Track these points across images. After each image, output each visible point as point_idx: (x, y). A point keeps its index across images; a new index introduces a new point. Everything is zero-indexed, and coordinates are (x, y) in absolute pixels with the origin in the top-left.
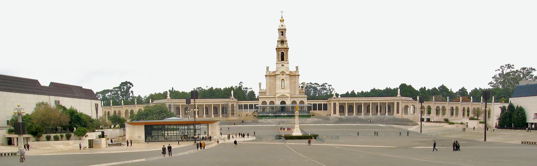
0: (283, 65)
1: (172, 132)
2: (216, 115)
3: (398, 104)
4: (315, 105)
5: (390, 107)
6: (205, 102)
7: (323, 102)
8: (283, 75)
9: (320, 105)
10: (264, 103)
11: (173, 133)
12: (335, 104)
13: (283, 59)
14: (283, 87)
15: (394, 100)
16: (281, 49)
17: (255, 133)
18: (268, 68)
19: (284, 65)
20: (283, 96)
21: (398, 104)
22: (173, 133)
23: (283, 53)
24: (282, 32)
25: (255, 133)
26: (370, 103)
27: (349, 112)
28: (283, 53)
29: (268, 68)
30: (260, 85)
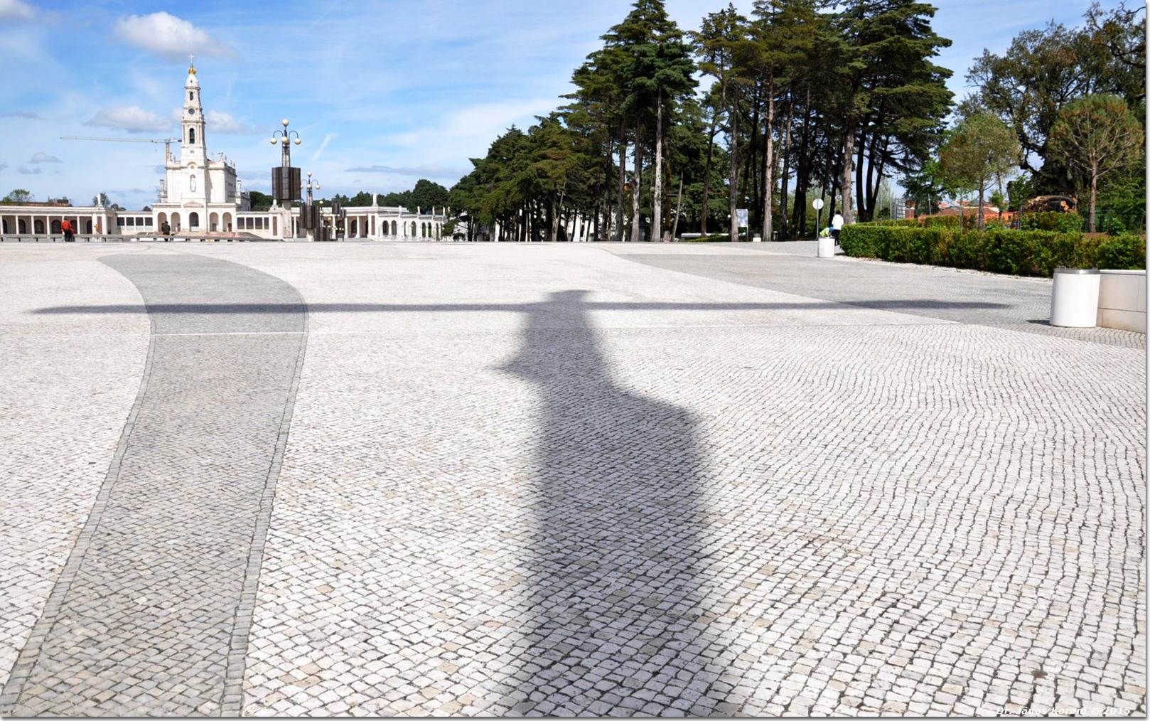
0: (192, 152)
3: (373, 217)
4: (250, 220)
7: (262, 215)
8: (192, 167)
9: (259, 220)
10: (162, 216)
12: (275, 219)
13: (192, 141)
15: (367, 212)
19: (195, 150)
20: (192, 204)
21: (373, 217)
23: (192, 130)
24: (191, 93)
28: (192, 130)
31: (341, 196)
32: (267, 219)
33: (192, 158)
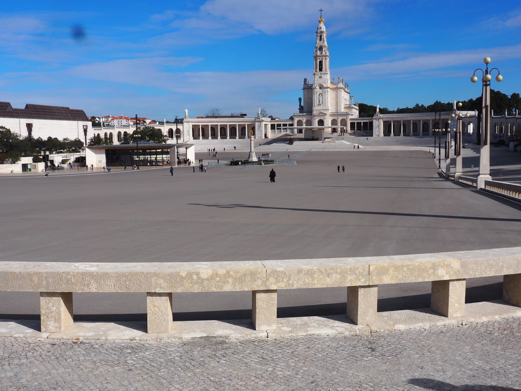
0: (321, 77)
1: (149, 156)
2: (214, 136)
5: (405, 125)
6: (228, 122)
11: (168, 157)
13: (321, 70)
14: (321, 102)
16: (319, 58)
17: (289, 156)
18: (305, 80)
22: (168, 157)
25: (289, 156)
26: (391, 121)
27: (231, 135)
28: (321, 62)
29: (305, 80)
30: (300, 99)
31: (420, 105)
32: (371, 124)
33: (321, 81)
